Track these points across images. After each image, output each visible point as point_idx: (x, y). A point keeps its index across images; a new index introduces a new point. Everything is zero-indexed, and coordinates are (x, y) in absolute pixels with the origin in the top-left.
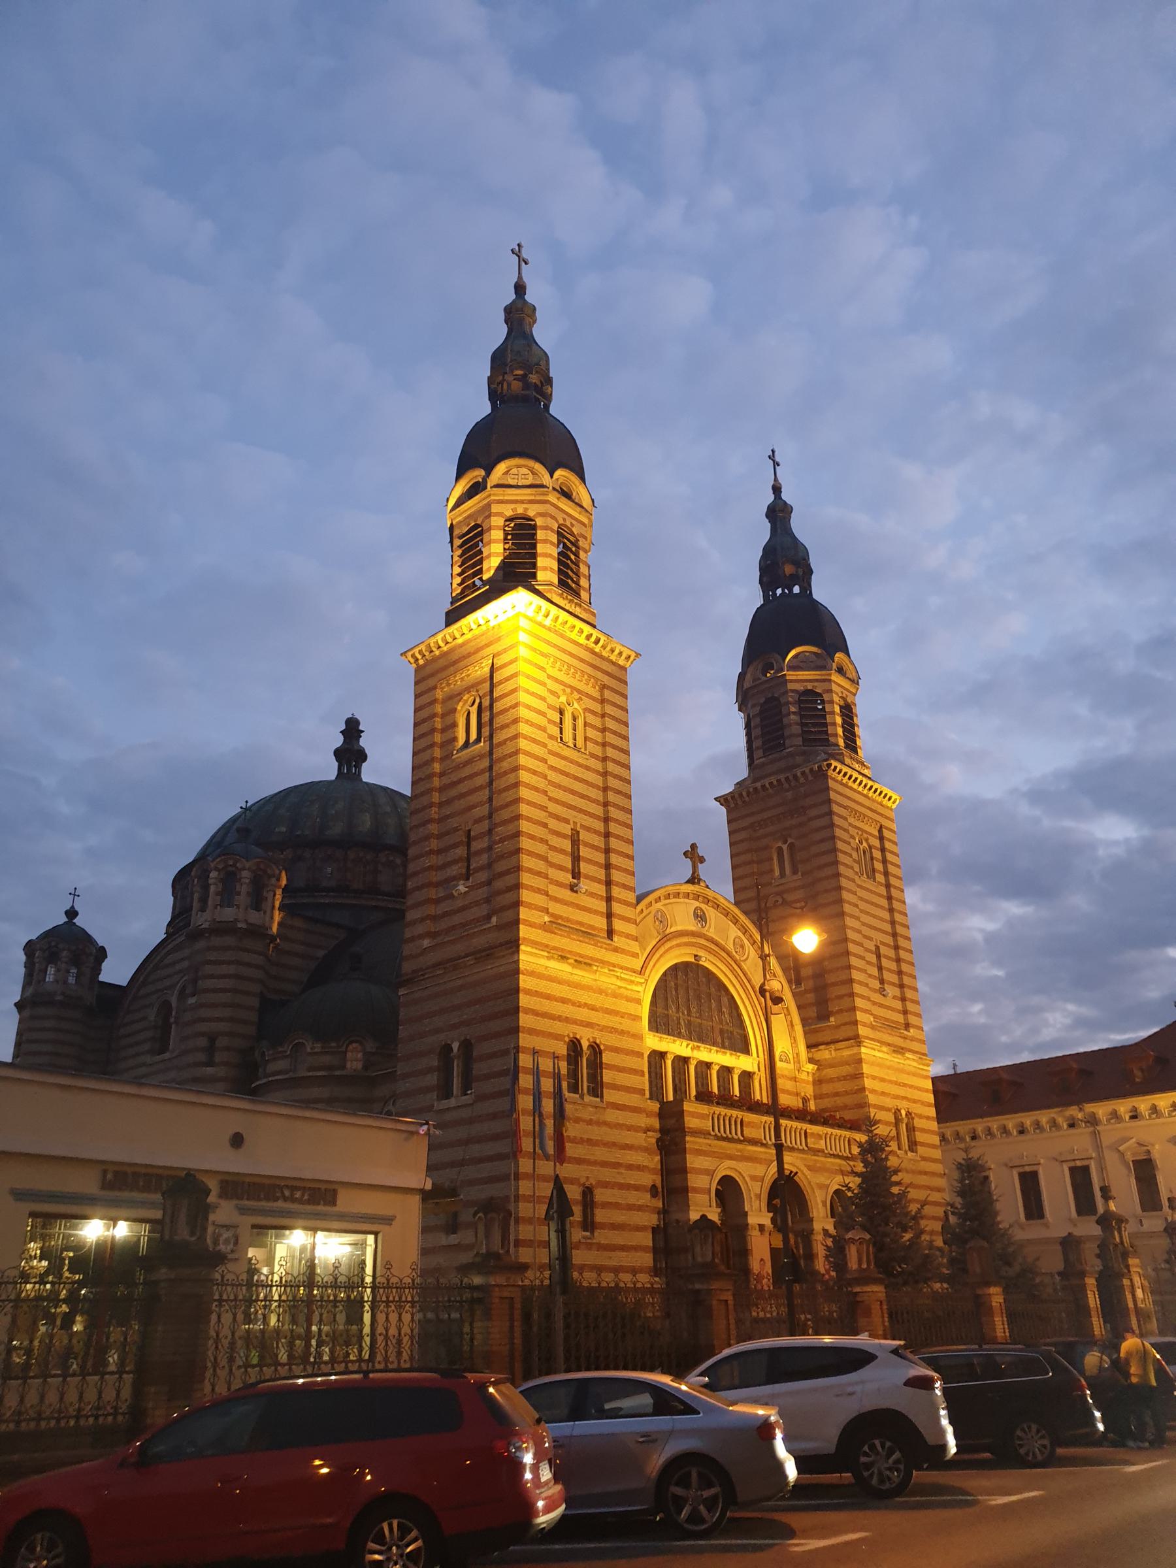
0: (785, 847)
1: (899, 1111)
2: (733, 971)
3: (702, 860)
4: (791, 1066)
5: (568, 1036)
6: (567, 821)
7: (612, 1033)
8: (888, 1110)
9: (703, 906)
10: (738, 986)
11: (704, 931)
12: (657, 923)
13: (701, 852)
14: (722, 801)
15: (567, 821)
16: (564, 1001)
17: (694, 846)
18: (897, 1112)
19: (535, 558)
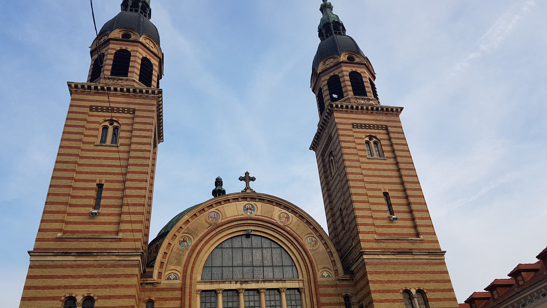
0: (332, 158)
1: (409, 291)
2: (278, 233)
3: (253, 179)
4: (334, 278)
5: (65, 296)
6: (94, 181)
7: (106, 288)
8: (397, 291)
9: (252, 203)
10: (284, 240)
11: (253, 216)
12: (211, 219)
13: (251, 175)
14: (311, 148)
15: (94, 181)
16: (64, 277)
17: (247, 173)
18: (407, 292)
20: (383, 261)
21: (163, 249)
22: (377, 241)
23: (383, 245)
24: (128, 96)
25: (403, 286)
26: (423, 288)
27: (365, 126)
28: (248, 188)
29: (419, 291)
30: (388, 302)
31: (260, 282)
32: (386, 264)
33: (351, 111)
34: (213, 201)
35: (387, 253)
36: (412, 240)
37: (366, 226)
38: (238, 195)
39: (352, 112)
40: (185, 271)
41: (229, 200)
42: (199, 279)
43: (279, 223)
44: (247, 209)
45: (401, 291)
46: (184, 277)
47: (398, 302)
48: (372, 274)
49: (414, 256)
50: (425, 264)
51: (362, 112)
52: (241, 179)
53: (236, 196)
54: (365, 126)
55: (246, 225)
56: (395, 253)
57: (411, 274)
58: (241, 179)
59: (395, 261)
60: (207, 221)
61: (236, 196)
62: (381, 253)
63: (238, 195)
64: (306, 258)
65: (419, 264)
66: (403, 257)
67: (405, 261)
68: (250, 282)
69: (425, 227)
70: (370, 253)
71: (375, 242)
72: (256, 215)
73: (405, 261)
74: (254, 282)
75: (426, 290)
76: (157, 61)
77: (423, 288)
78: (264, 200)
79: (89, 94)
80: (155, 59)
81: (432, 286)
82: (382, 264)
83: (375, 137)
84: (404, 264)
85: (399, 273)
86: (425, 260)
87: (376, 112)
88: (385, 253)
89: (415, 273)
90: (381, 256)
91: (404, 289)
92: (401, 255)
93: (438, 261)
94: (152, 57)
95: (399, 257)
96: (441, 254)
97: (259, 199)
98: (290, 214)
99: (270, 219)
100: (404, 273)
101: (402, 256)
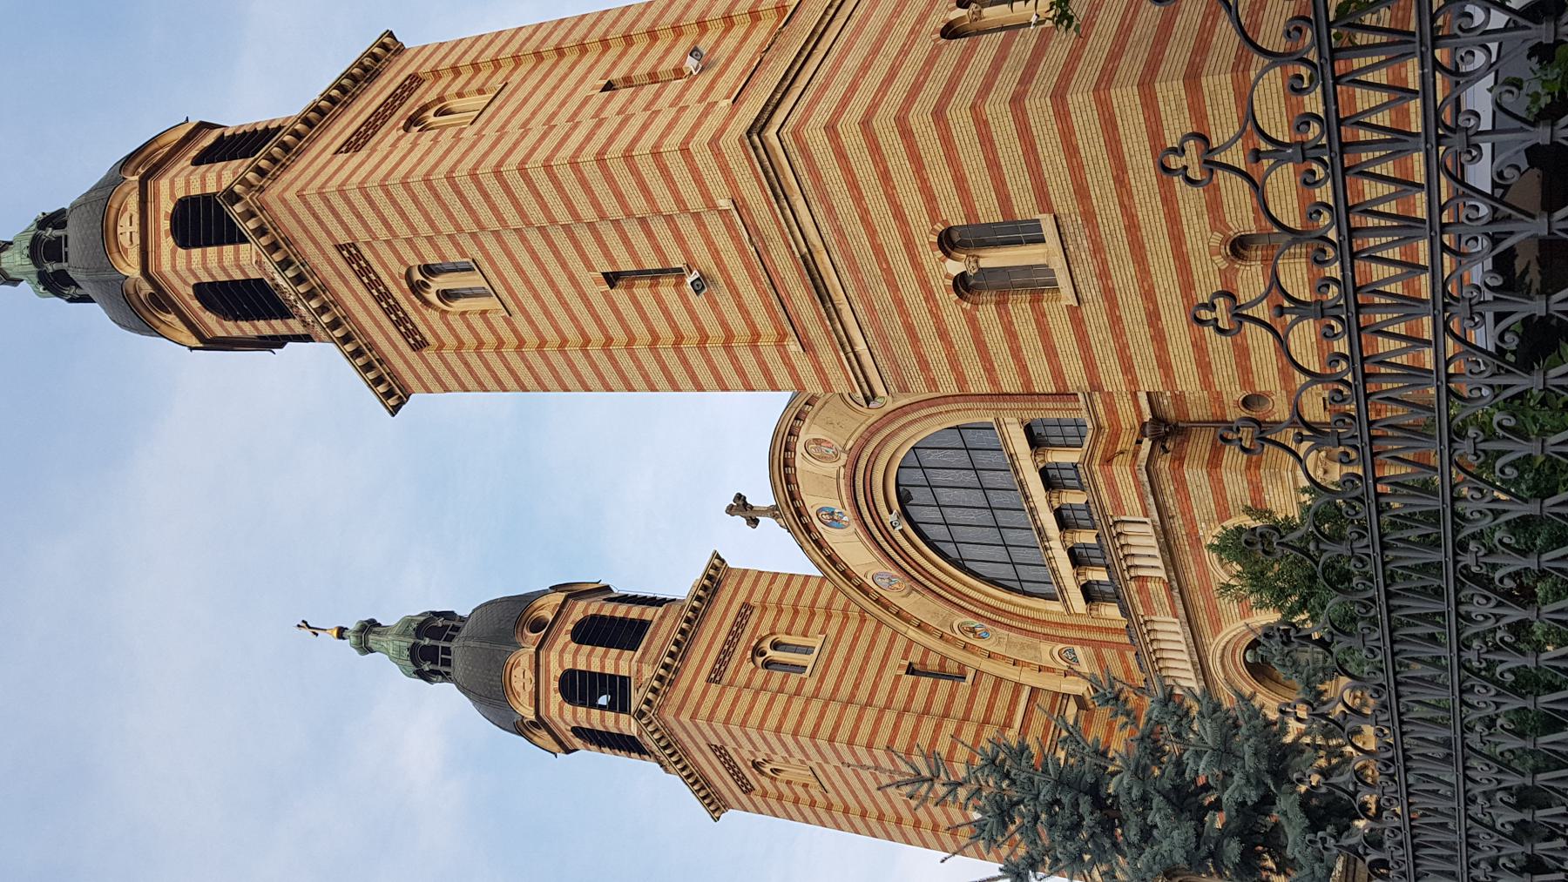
8: (972, 322)
12: (897, 586)
17: (730, 510)
19: (605, 675)
20: (875, 345)
21: (1010, 673)
22: (806, 346)
23: (815, 332)
24: (684, 749)
25: (948, 301)
26: (930, 233)
27: (401, 321)
28: (773, 512)
29: (948, 242)
30: (1019, 349)
31: (1032, 505)
32: (882, 336)
33: (370, 351)
34: (848, 589)
35: (842, 333)
36: (750, 239)
37: (768, 370)
38: (806, 544)
39: (372, 346)
40: (1048, 637)
41: (829, 557)
42: (1056, 607)
43: (842, 462)
44: (833, 519)
45: (965, 305)
46: (1062, 639)
47: (1011, 323)
48: (933, 380)
49: (814, 246)
50: (830, 210)
51: (344, 318)
52: (754, 522)
53: (810, 548)
54: (401, 321)
55: (880, 524)
56: (832, 309)
57: (887, 263)
58: (754, 522)
59: (859, 307)
60: (904, 593)
61: (810, 548)
62: (849, 349)
63: (806, 544)
64: (924, 412)
65: (840, 232)
66: (832, 281)
67: (846, 276)
68: (1039, 523)
69: (674, 183)
70: (862, 379)
71: (814, 351)
72: (844, 507)
73: (846, 276)
74: (1037, 517)
75: (933, 222)
76: (548, 656)
77: (930, 233)
78: (791, 493)
79: (718, 792)
80: (548, 664)
81: (912, 203)
82: (887, 348)
83: (408, 276)
84: (858, 281)
85: (900, 303)
86: (815, 209)
87: (312, 277)
88: (845, 339)
89: (878, 251)
90: (857, 349)
91: (954, 296)
92: (829, 288)
93: (799, 163)
94: (548, 671)
95: (839, 297)
96: (761, 151)
97: (793, 499)
98: (804, 436)
99: (842, 482)
100: (893, 286)
101: (833, 286)
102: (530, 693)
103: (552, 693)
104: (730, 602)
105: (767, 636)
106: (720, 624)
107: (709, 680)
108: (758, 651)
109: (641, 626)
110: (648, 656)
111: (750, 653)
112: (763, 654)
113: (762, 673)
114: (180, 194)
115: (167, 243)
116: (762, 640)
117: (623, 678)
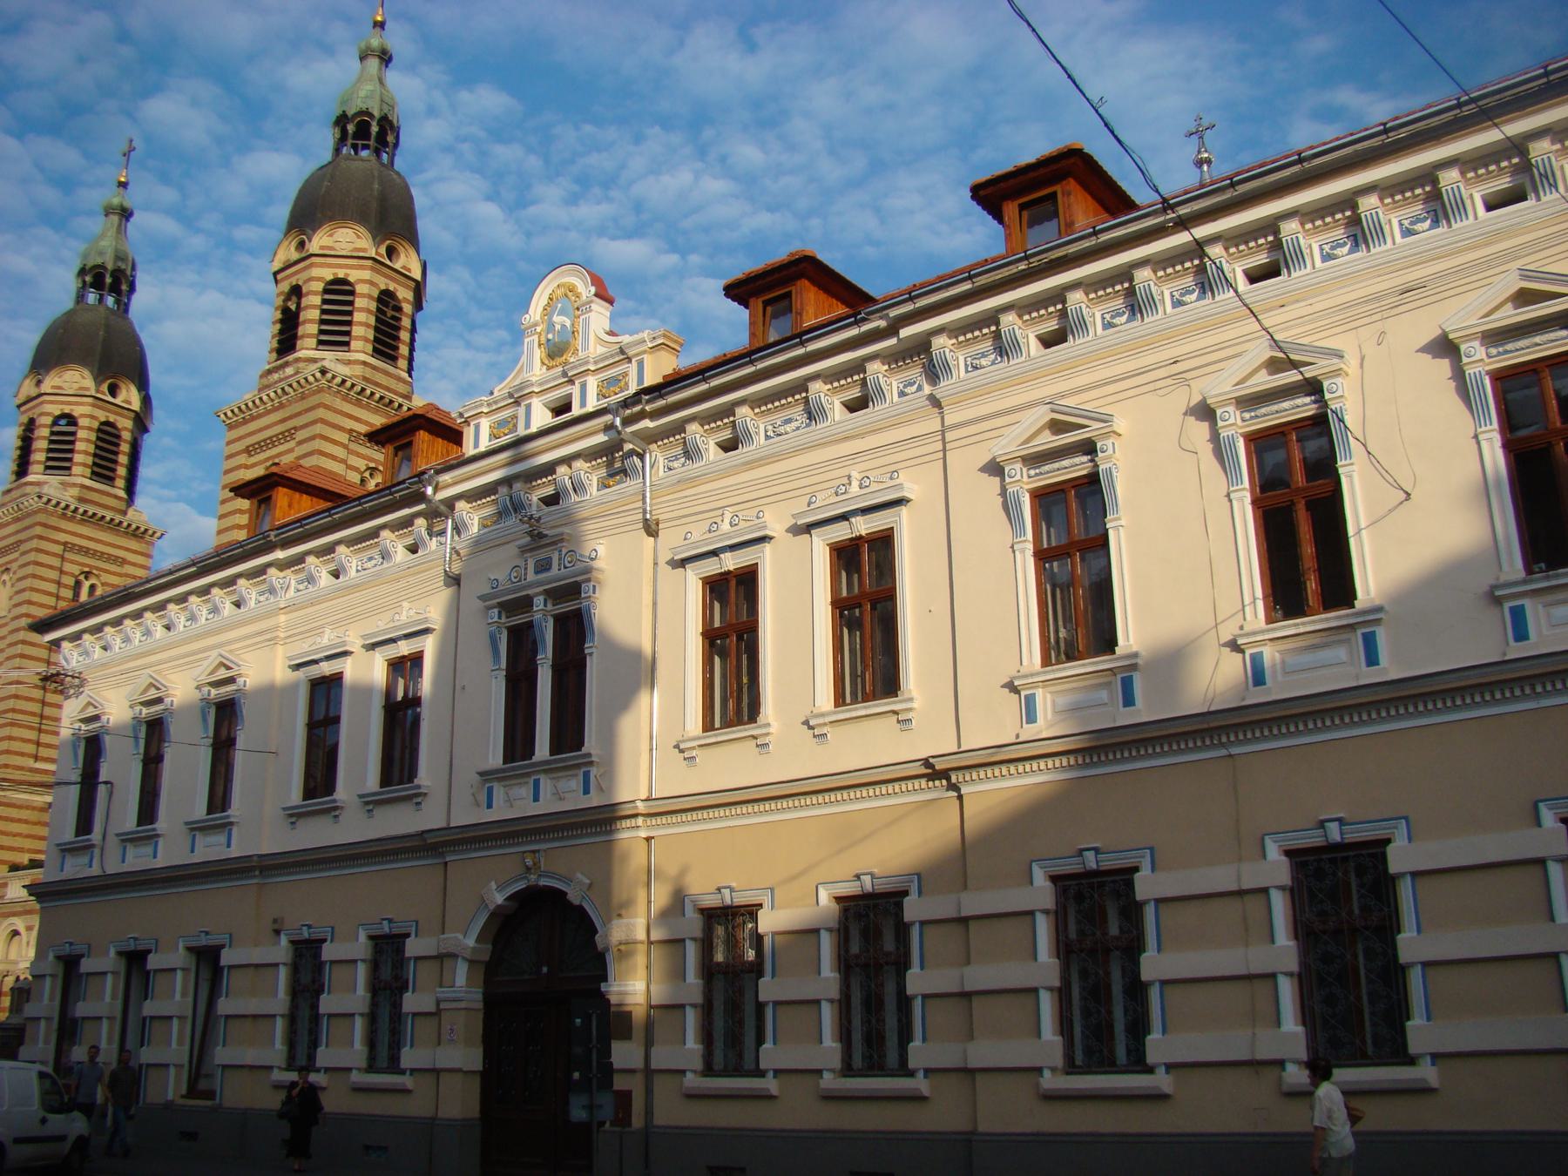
102: (60, 388)
103: (61, 407)
104: (127, 549)
105: (100, 581)
106: (109, 544)
107: (65, 544)
108: (87, 575)
109: (110, 480)
110: (85, 491)
111: (87, 569)
112: (86, 578)
113: (70, 581)
114: (360, 289)
115: (328, 275)
116: (98, 576)
117: (69, 469)
